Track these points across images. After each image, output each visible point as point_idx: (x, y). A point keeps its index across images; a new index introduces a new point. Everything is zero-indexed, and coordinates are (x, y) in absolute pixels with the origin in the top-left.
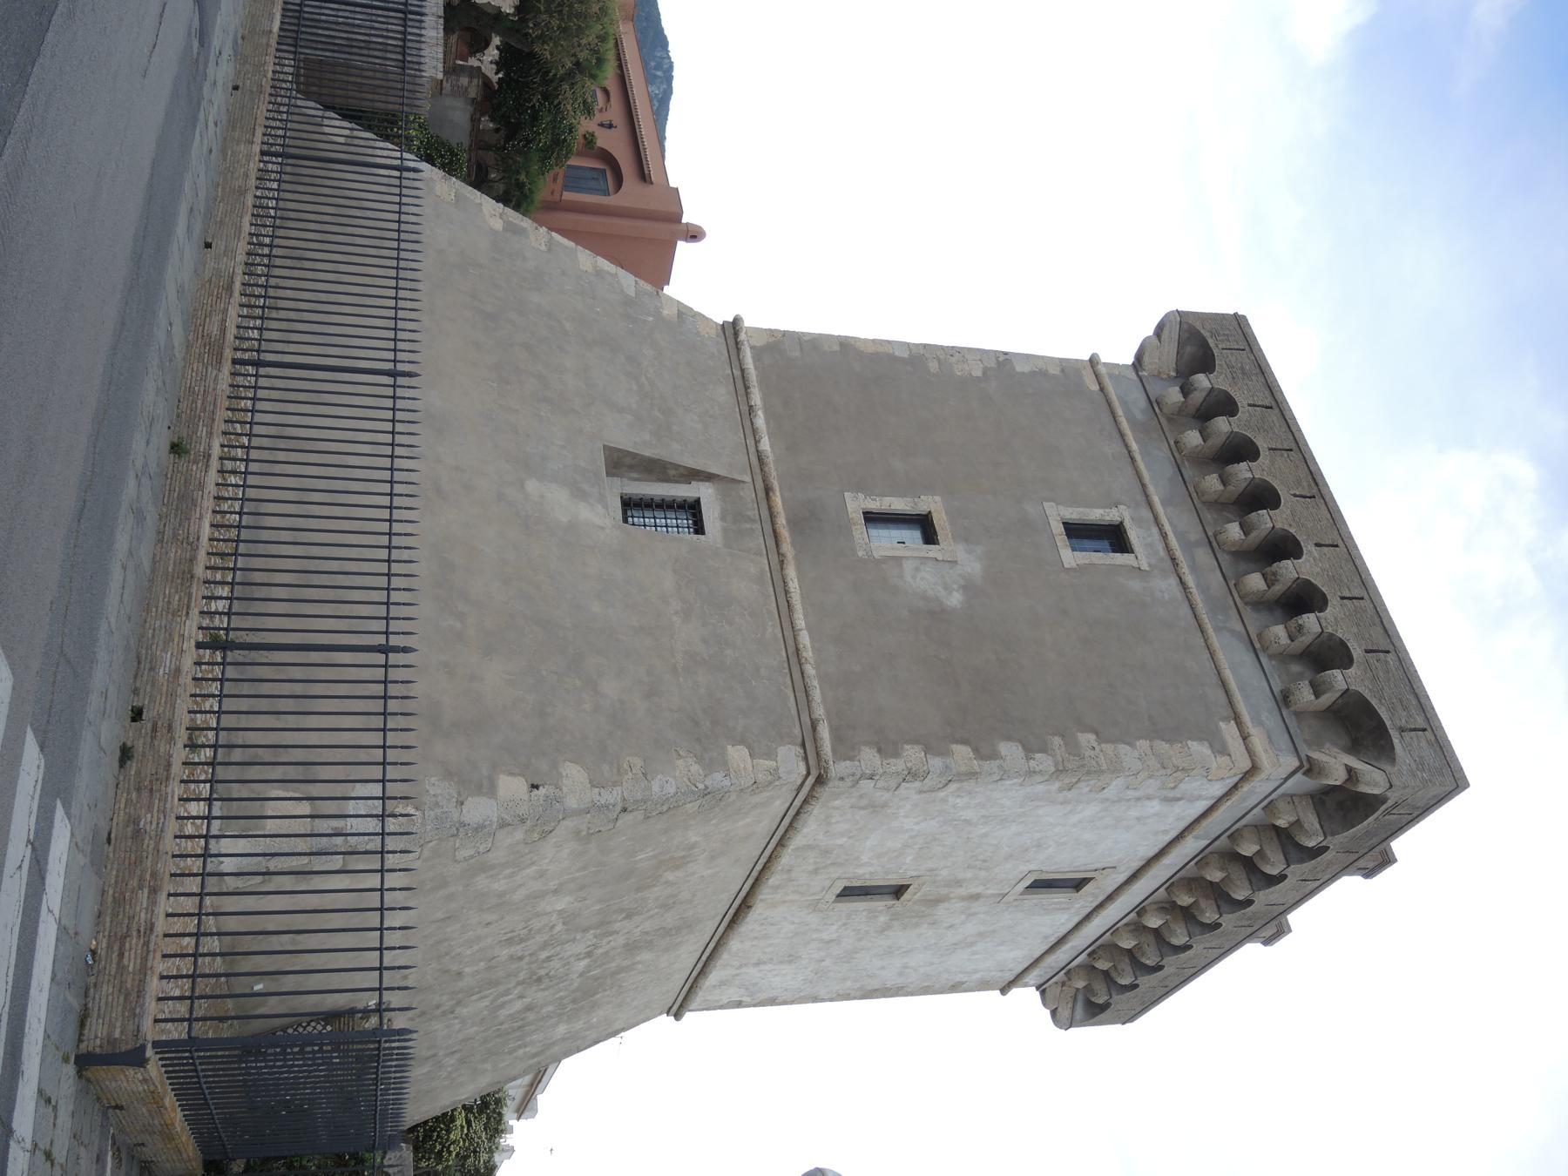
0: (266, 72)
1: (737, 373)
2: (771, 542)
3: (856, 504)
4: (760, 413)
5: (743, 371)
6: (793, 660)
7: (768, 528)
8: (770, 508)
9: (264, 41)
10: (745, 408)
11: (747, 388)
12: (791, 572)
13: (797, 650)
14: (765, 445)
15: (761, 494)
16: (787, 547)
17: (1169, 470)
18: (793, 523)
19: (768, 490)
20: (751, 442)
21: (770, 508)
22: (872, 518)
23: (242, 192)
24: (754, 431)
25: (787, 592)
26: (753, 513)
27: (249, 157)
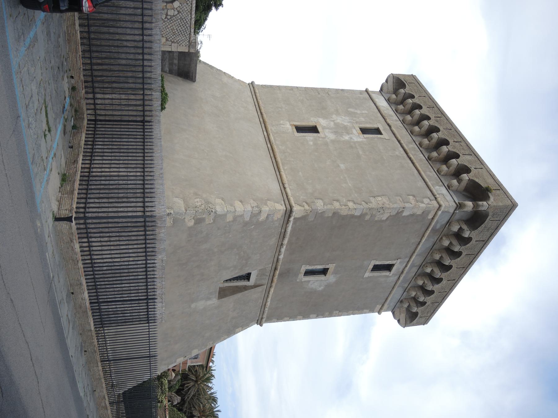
0: (95, 346)
1: (283, 230)
2: (270, 281)
3: (304, 268)
4: (285, 247)
5: (285, 231)
6: (263, 306)
7: (271, 278)
8: (274, 273)
9: (90, 334)
10: (280, 243)
11: (284, 237)
12: (272, 290)
13: (265, 305)
14: (281, 257)
15: (273, 269)
16: (274, 284)
17: (430, 244)
18: (280, 275)
19: (276, 269)
20: (277, 254)
21: (274, 273)
22: (308, 273)
23: (100, 379)
24: (280, 251)
25: (269, 293)
26: (268, 274)
27: (99, 371)
